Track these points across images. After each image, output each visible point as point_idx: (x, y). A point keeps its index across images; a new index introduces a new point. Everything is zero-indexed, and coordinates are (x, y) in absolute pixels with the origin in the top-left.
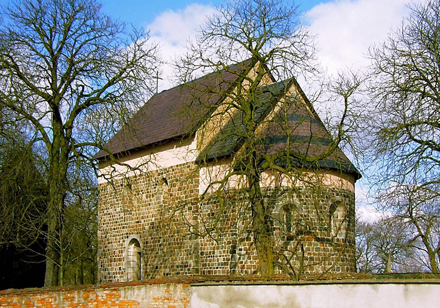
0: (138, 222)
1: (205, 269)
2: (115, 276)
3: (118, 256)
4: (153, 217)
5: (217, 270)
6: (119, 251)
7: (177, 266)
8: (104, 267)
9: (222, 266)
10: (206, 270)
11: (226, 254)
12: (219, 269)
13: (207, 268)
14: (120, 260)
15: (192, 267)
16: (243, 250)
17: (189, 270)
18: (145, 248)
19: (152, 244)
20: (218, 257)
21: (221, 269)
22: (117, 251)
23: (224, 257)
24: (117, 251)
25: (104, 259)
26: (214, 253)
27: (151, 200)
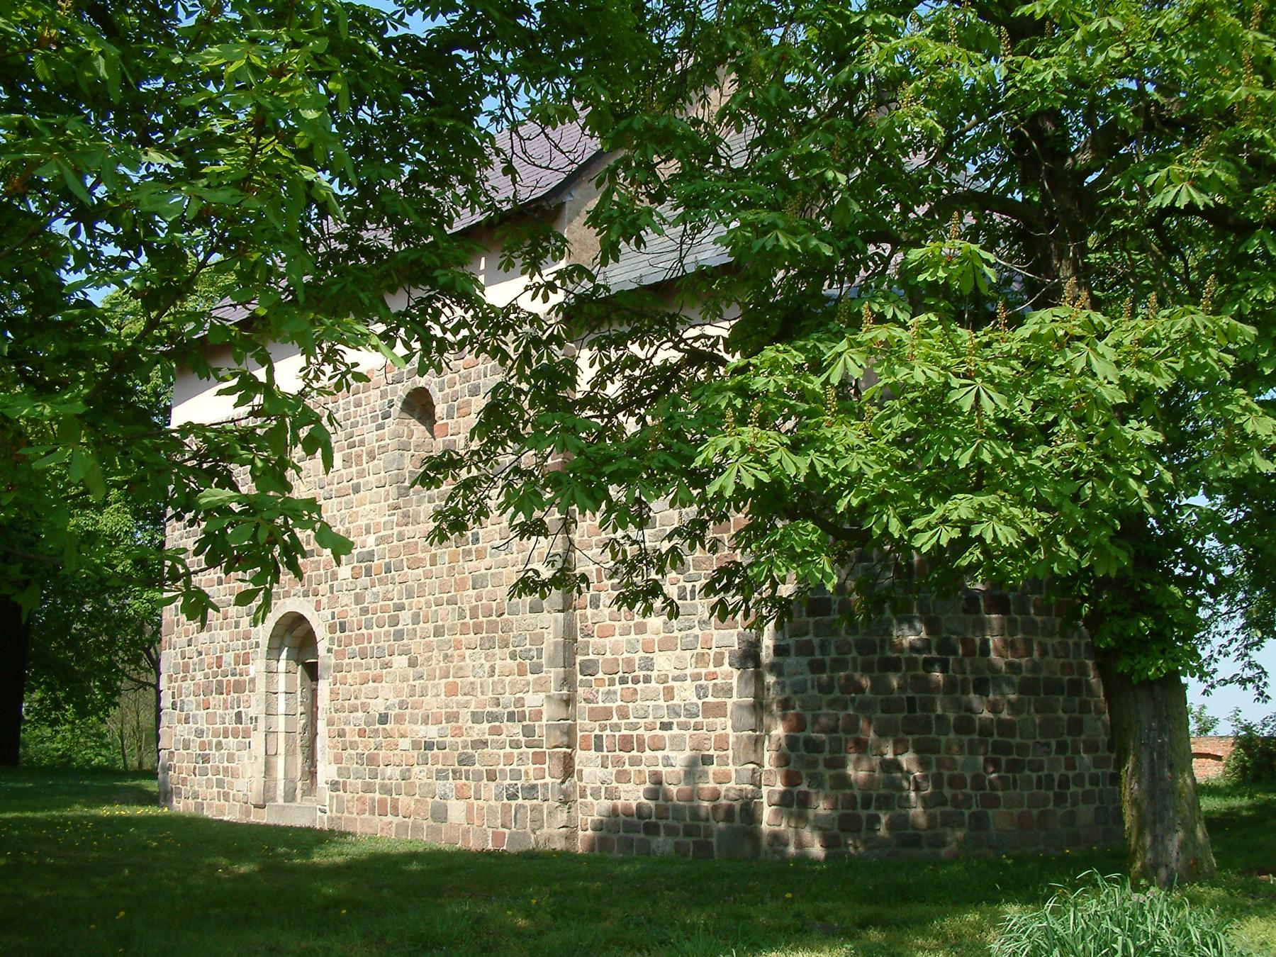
1: (603, 728)
2: (219, 743)
3: (234, 675)
4: (368, 532)
5: (666, 734)
6: (237, 656)
7: (473, 714)
8: (182, 710)
9: (692, 721)
10: (608, 732)
11: (711, 668)
12: (675, 731)
13: (616, 727)
14: (239, 687)
15: (544, 722)
16: (793, 651)
17: (529, 731)
18: (335, 647)
19: (363, 631)
20: (671, 683)
21: (687, 733)
22: (229, 657)
23: (703, 682)
24: (229, 657)
25: (185, 685)
26: (648, 665)
27: (361, 474)
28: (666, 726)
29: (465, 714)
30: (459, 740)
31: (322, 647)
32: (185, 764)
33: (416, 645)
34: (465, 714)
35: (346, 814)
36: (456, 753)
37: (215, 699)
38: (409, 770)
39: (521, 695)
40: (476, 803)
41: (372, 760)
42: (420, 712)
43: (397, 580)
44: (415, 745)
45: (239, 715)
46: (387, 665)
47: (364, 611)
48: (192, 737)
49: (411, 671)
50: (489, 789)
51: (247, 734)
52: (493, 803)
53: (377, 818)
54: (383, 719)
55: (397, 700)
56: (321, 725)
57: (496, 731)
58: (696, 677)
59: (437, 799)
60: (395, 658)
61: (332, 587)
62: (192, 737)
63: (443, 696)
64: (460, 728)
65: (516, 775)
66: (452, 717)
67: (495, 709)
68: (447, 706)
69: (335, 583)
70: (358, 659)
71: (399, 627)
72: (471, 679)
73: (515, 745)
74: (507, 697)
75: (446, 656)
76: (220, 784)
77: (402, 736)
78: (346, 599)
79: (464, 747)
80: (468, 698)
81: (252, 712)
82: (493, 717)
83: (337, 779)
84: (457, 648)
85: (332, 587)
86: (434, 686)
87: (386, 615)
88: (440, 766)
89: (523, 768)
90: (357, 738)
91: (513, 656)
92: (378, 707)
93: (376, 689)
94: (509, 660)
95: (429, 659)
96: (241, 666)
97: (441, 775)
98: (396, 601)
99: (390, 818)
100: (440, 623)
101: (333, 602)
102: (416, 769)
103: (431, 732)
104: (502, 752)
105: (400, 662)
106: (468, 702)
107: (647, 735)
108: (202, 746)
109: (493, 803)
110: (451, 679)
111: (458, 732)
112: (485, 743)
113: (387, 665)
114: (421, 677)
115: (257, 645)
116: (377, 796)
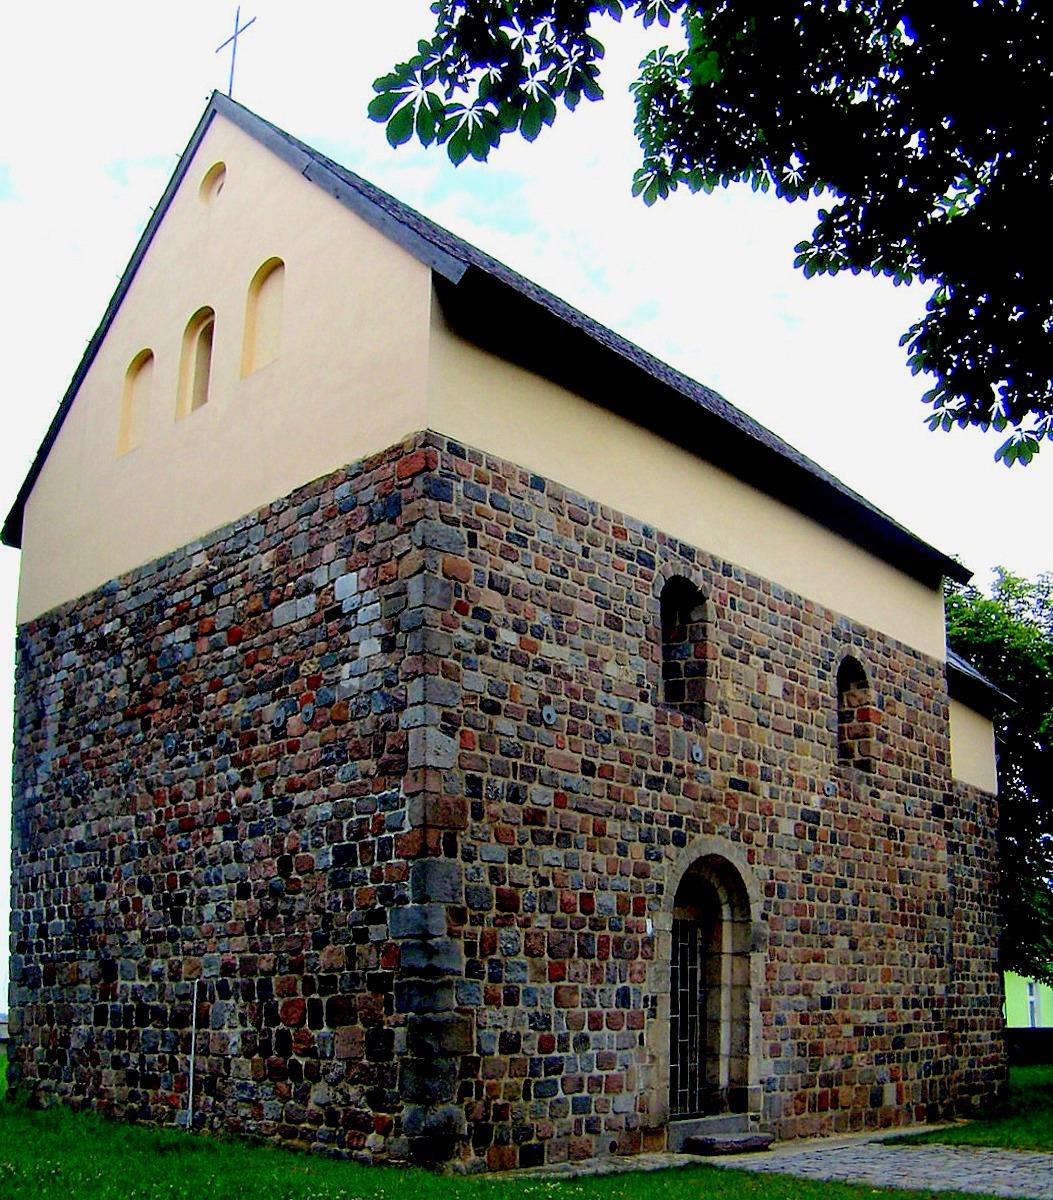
0: (742, 786)
4: (812, 789)
17: (936, 1016)
18: (771, 914)
22: (605, 899)
28: (976, 1013)
29: (898, 1000)
30: (894, 1024)
31: (756, 909)
32: (506, 1080)
33: (857, 927)
34: (898, 1000)
35: (783, 1118)
36: (893, 1037)
37: (577, 965)
38: (851, 1058)
39: (931, 985)
40: (905, 1083)
41: (815, 1049)
42: (862, 998)
43: (841, 854)
44: (858, 1031)
45: (624, 997)
46: (830, 945)
47: (807, 879)
48: (525, 1030)
49: (850, 954)
50: (913, 1069)
51: (636, 1023)
52: (916, 1081)
53: (816, 1115)
54: (826, 1003)
55: (839, 984)
56: (754, 1011)
57: (917, 1016)
58: (987, 979)
59: (875, 1084)
60: (838, 937)
61: (770, 839)
62: (525, 1030)
63: (880, 982)
64: (894, 1013)
65: (930, 1054)
66: (889, 1003)
67: (916, 996)
68: (885, 992)
69: (775, 835)
70: (798, 933)
71: (840, 905)
72: (899, 967)
73: (928, 1028)
74: (923, 987)
75: (881, 943)
76: (581, 1106)
77: (847, 1021)
78: (786, 858)
79: (899, 1031)
80: (899, 984)
81: (647, 989)
82: (916, 1003)
83: (774, 1076)
84: (890, 936)
85: (770, 839)
86: (873, 971)
87: (829, 889)
88: (878, 1051)
89: (934, 1048)
90: (799, 1025)
91: (927, 951)
92: (821, 989)
93: (818, 970)
94: (924, 954)
95: (867, 944)
96: (630, 916)
97: (879, 1060)
98: (838, 875)
99: (830, 1112)
100: (876, 909)
101: (770, 855)
102: (857, 1056)
103: (869, 1017)
104: (921, 1035)
105: (842, 942)
106: (900, 988)
108: (546, 1045)
109: (916, 1081)
110: (885, 965)
111: (892, 1018)
113: (830, 945)
114: (861, 962)
115: (660, 888)
116: (818, 1089)
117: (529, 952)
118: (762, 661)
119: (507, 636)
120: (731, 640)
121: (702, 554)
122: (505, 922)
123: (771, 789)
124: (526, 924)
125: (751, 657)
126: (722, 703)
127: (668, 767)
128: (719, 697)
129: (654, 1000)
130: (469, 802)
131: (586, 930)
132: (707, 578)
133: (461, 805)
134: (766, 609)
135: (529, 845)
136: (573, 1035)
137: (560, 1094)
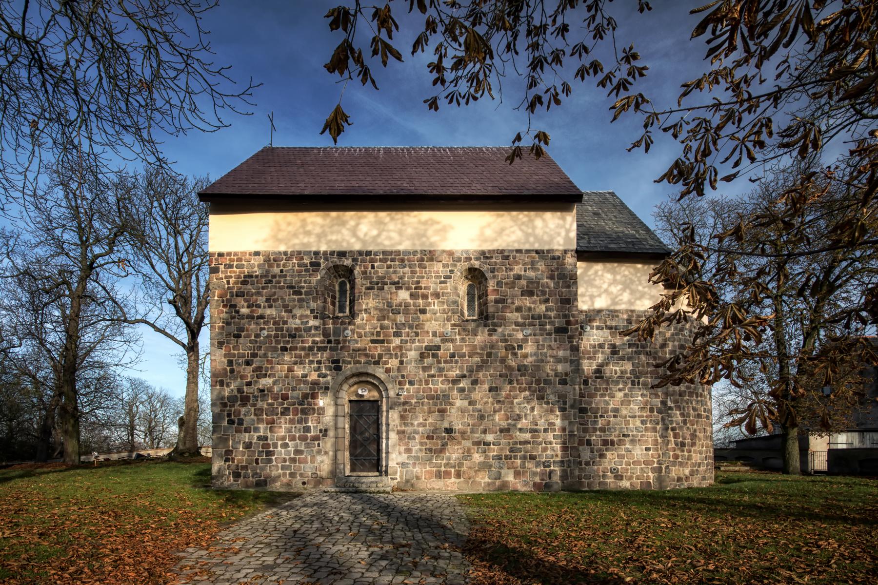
49: (471, 408)
107: (615, 439)
112: (529, 442)
117: (255, 415)
118: (393, 286)
119: (245, 311)
120: (371, 283)
121: (351, 252)
122: (244, 405)
123: (402, 340)
124: (254, 405)
125: (386, 287)
126: (366, 310)
127: (329, 342)
128: (364, 307)
129: (326, 430)
130: (228, 368)
131: (285, 406)
132: (355, 260)
133: (225, 369)
134: (397, 263)
135: (255, 379)
136: (280, 443)
137: (274, 463)
